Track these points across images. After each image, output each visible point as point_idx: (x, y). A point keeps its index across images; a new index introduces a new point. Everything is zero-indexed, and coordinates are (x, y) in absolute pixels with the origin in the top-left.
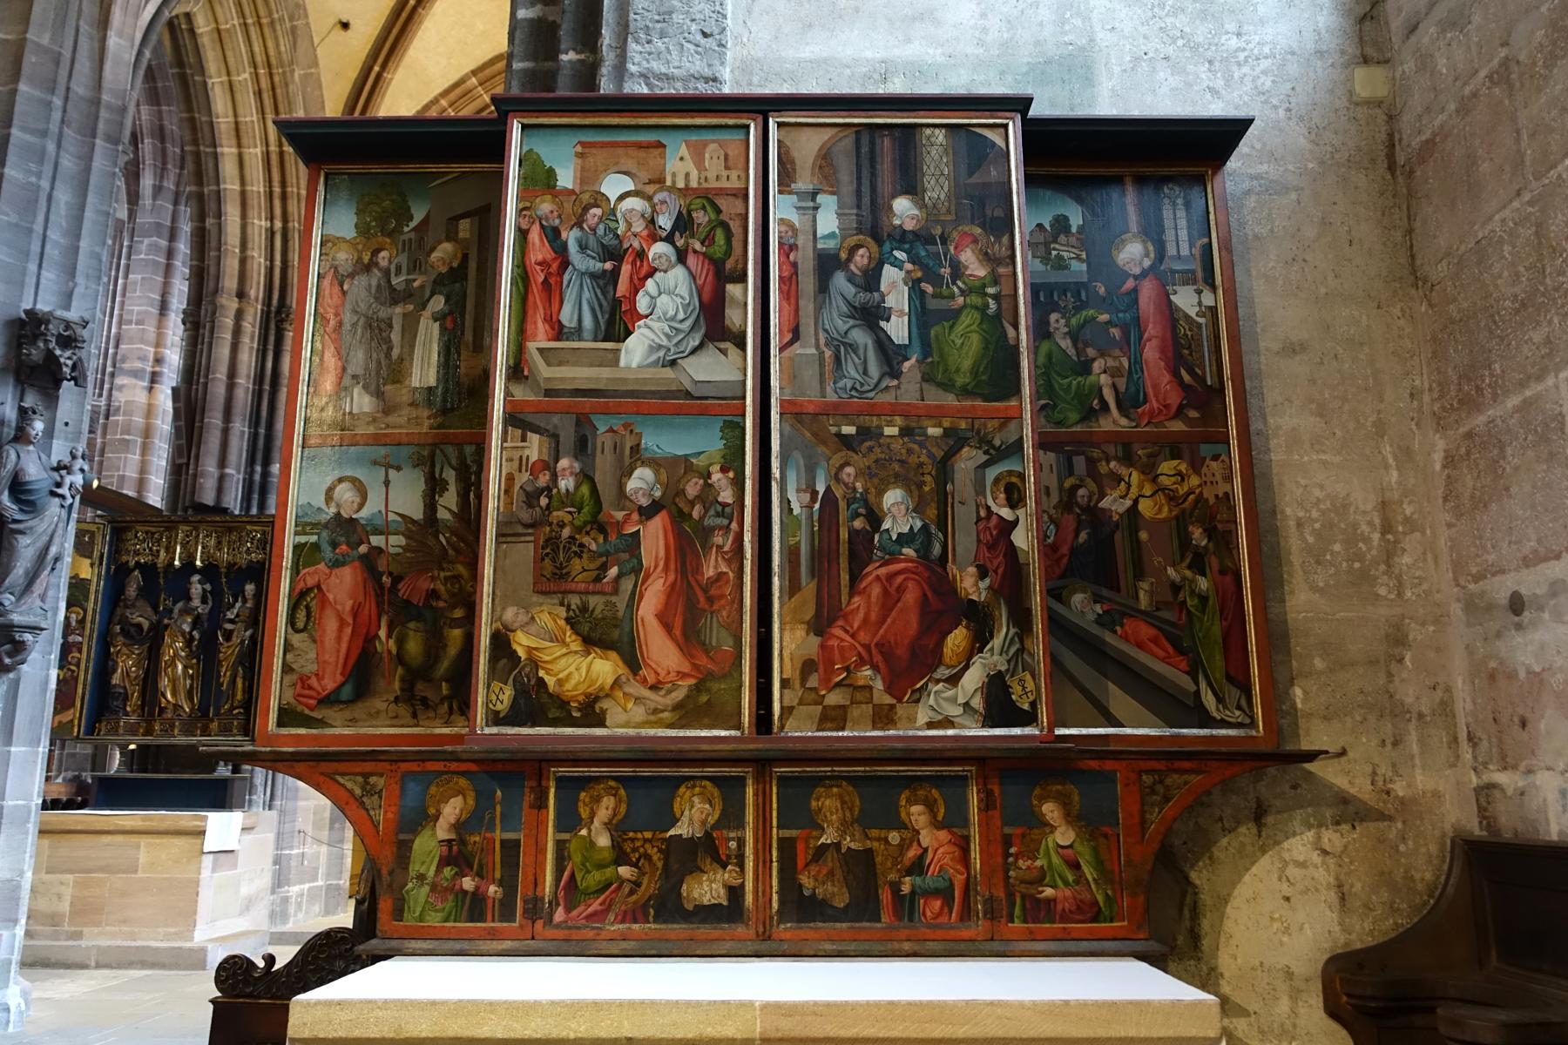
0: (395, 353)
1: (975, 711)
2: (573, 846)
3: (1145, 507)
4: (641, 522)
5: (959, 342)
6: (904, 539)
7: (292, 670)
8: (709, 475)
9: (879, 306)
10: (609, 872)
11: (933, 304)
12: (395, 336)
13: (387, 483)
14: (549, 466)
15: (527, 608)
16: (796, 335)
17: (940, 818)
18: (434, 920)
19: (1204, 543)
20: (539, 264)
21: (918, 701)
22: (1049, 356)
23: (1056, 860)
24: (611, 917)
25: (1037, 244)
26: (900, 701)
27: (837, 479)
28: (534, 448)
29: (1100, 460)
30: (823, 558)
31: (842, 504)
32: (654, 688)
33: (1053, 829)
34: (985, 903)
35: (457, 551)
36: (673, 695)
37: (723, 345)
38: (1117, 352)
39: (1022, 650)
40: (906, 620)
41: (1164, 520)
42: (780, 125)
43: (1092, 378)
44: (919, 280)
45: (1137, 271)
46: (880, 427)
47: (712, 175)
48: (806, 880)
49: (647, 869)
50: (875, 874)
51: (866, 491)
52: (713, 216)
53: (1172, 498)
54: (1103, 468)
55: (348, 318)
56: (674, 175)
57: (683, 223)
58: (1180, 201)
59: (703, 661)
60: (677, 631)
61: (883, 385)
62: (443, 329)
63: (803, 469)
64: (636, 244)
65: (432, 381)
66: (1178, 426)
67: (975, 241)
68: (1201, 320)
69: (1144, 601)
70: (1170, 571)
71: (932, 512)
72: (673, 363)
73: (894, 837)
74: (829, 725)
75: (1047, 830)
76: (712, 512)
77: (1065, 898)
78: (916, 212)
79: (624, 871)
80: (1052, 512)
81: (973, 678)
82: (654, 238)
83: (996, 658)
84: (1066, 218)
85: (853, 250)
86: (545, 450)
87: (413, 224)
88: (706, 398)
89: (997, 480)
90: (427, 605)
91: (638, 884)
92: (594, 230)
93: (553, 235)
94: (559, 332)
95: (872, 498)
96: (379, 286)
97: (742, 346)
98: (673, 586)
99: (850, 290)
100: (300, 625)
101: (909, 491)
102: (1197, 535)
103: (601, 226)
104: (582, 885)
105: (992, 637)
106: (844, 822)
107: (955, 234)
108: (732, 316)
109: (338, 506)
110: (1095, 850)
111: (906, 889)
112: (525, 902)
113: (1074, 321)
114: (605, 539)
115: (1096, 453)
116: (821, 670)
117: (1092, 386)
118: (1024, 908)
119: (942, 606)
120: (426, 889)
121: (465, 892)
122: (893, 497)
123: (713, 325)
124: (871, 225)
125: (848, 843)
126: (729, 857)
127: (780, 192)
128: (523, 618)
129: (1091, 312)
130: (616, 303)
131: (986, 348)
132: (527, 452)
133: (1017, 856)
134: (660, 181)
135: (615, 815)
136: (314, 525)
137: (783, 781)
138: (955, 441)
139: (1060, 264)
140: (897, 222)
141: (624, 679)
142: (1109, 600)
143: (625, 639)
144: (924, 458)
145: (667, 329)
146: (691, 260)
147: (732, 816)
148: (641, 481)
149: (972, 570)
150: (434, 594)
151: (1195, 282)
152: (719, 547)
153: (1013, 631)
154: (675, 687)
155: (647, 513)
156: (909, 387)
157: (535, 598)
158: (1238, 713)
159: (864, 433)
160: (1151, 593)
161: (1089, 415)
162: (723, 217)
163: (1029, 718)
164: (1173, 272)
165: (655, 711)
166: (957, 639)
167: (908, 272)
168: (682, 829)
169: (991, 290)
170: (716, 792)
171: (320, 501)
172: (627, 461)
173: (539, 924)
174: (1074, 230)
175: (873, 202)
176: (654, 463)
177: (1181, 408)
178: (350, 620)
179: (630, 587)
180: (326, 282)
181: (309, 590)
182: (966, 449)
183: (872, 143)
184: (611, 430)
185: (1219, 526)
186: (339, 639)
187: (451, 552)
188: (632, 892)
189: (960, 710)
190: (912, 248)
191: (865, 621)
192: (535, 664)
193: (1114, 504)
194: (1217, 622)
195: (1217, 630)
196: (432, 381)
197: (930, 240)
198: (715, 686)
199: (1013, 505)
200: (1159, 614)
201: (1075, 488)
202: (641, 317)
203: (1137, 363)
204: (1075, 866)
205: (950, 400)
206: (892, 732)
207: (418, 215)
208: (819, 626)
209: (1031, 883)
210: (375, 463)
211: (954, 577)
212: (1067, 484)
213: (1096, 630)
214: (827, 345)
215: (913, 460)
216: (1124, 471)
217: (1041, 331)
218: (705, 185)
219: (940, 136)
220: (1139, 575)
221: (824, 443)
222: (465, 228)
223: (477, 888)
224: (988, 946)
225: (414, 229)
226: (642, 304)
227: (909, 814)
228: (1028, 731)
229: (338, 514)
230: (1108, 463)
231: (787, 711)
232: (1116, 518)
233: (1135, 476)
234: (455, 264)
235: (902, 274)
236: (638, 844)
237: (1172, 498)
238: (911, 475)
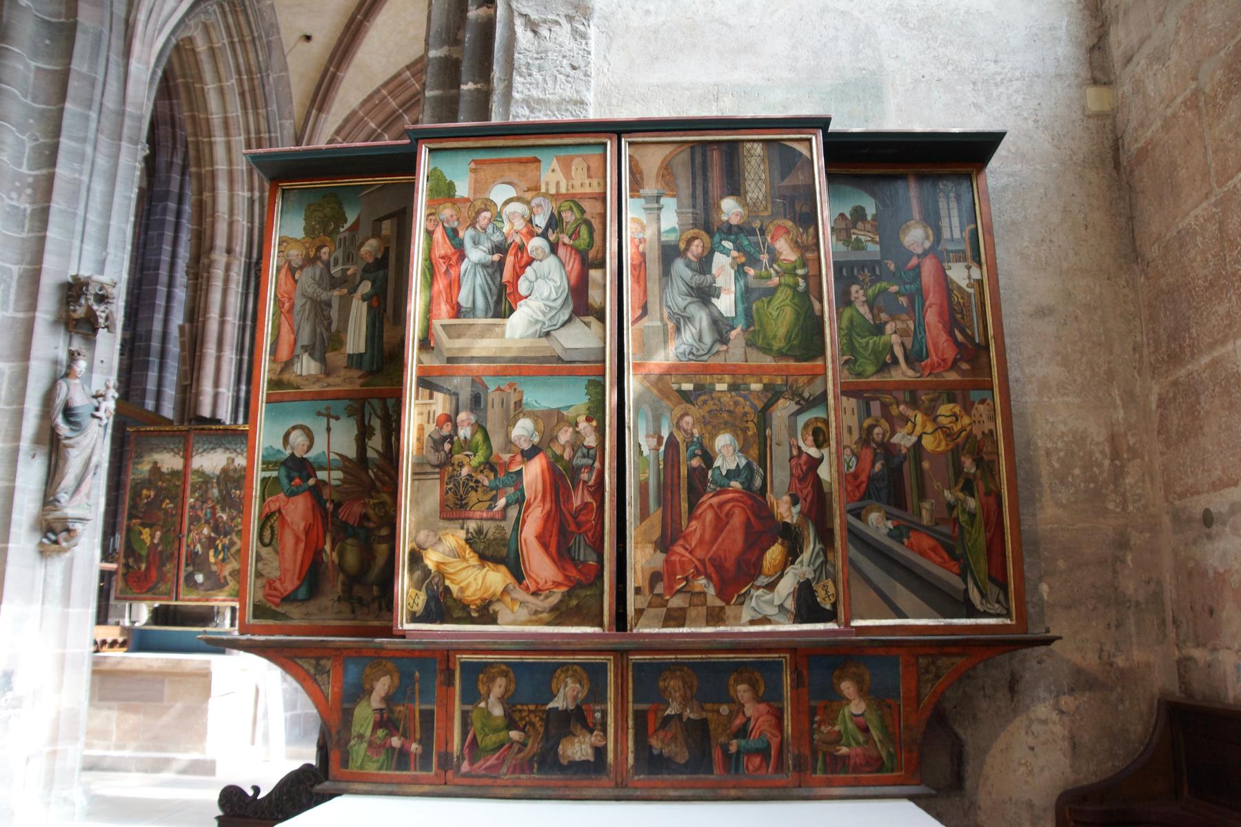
0: (334, 327)
1: (788, 611)
2: (475, 715)
3: (928, 442)
4: (523, 462)
5: (775, 314)
6: (731, 475)
7: (262, 575)
8: (577, 425)
9: (710, 286)
10: (502, 734)
11: (753, 283)
12: (334, 314)
13: (329, 429)
14: (450, 419)
15: (435, 530)
16: (645, 311)
17: (761, 693)
18: (372, 768)
19: (973, 471)
20: (443, 258)
21: (742, 604)
22: (851, 320)
23: (850, 726)
24: (504, 769)
25: (840, 230)
26: (728, 603)
27: (678, 426)
28: (440, 404)
29: (891, 404)
30: (667, 489)
31: (682, 447)
32: (535, 594)
33: (849, 701)
34: (794, 759)
36: (551, 599)
37: (587, 319)
38: (905, 317)
39: (825, 562)
40: (734, 540)
41: (942, 453)
42: (630, 144)
43: (884, 339)
44: (743, 265)
45: (919, 251)
46: (713, 384)
47: (577, 183)
48: (655, 743)
49: (532, 732)
50: (709, 739)
51: (702, 435)
52: (578, 215)
53: (949, 434)
54: (894, 411)
55: (299, 302)
56: (547, 184)
57: (555, 222)
58: (952, 195)
59: (573, 573)
60: (553, 549)
61: (715, 350)
62: (370, 308)
63: (651, 419)
64: (518, 240)
65: (362, 350)
66: (952, 376)
67: (788, 232)
68: (971, 291)
69: (926, 518)
70: (947, 493)
71: (754, 452)
72: (548, 334)
73: (724, 710)
74: (672, 623)
75: (844, 702)
76: (579, 454)
77: (857, 755)
78: (740, 210)
79: (514, 735)
80: (854, 447)
81: (787, 585)
82: (532, 234)
83: (805, 568)
84: (863, 209)
85: (689, 242)
86: (448, 406)
87: (347, 226)
88: (574, 362)
89: (806, 426)
90: (361, 525)
91: (524, 745)
92: (484, 229)
93: (453, 234)
94: (457, 311)
95: (706, 442)
96: (321, 275)
97: (601, 318)
98: (548, 515)
99: (687, 274)
100: (267, 540)
101: (736, 436)
102: (968, 465)
103: (490, 227)
104: (482, 744)
105: (802, 552)
106: (684, 698)
107: (771, 227)
108: (594, 296)
109: (293, 448)
110: (882, 719)
111: (733, 749)
112: (439, 756)
113: (870, 292)
114: (495, 476)
115: (888, 399)
116: (665, 579)
117: (885, 344)
118: (824, 762)
119: (764, 528)
120: (365, 745)
121: (394, 749)
122: (723, 441)
123: (580, 303)
124: (706, 222)
125: (689, 714)
126: (595, 725)
127: (631, 197)
128: (432, 539)
129: (884, 284)
130: (502, 288)
131: (797, 319)
132: (433, 407)
133: (820, 724)
134: (537, 188)
135: (506, 692)
136: (276, 464)
137: (638, 666)
138: (773, 394)
139: (859, 246)
140: (724, 218)
141: (511, 587)
142: (898, 517)
143: (512, 556)
144: (747, 409)
145: (543, 308)
146: (562, 251)
147: (597, 694)
148: (523, 430)
149: (786, 498)
150: (365, 517)
151: (965, 260)
152: (585, 482)
153: (818, 546)
154: (551, 593)
155: (529, 455)
156: (736, 352)
157: (442, 523)
158: (997, 606)
159: (699, 388)
160: (932, 512)
161: (883, 367)
162: (587, 216)
163: (831, 616)
164: (948, 252)
165: (536, 612)
166: (774, 553)
167: (734, 258)
168: (558, 703)
169: (800, 272)
170: (585, 676)
171: (279, 445)
172: (512, 413)
173: (450, 774)
174: (869, 218)
175: (706, 202)
176: (534, 415)
177: (955, 362)
178: (303, 537)
179: (515, 514)
180: (283, 271)
181: (273, 514)
182: (781, 401)
183: (704, 155)
184: (499, 389)
185: (985, 457)
186: (295, 551)
187: (378, 483)
188: (520, 751)
189: (777, 610)
190: (737, 239)
191: (701, 541)
192: (442, 575)
193: (903, 439)
194: (983, 534)
195: (982, 541)
196: (362, 350)
197: (752, 232)
198: (583, 593)
199: (819, 445)
200: (937, 528)
201: (872, 427)
202: (522, 298)
203: (921, 325)
204: (865, 730)
205: (768, 361)
206: (722, 629)
207: (351, 218)
208: (665, 544)
209: (831, 743)
210: (319, 414)
211: (772, 504)
212: (866, 424)
213: (889, 542)
214: (669, 318)
215: (739, 410)
216: (910, 413)
217: (844, 300)
218: (572, 191)
219: (758, 149)
220: (922, 496)
221: (668, 398)
222: (387, 227)
223: (403, 746)
224: (796, 792)
225: (348, 230)
226: (523, 287)
227: (736, 691)
228: (831, 626)
229: (293, 455)
230: (898, 405)
231: (639, 612)
232: (904, 451)
233: (920, 418)
234: (379, 256)
235: (729, 260)
236: (524, 714)
237: (949, 434)
238: (737, 423)
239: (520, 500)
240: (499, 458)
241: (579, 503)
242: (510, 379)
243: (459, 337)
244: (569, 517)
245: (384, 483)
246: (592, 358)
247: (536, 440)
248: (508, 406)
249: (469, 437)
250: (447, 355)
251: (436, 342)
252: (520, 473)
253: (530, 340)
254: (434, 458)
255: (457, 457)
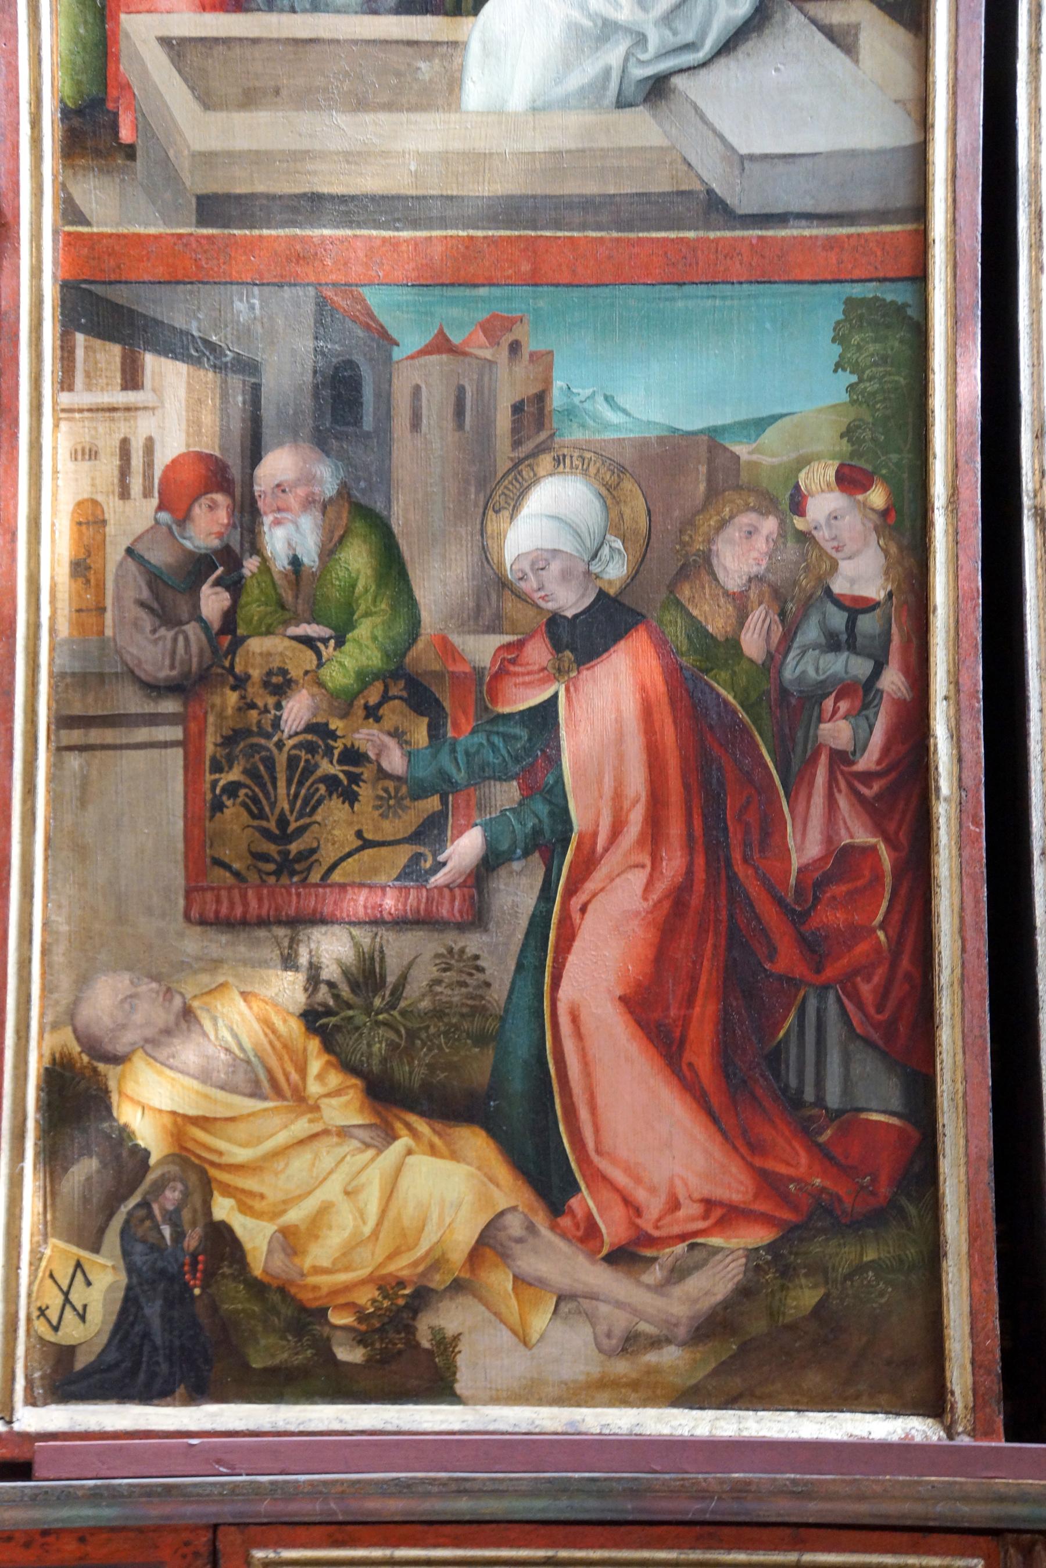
4: (560, 672)
8: (798, 504)
14: (224, 476)
15: (164, 976)
28: (176, 411)
32: (624, 1257)
59: (795, 1162)
60: (701, 1056)
72: (657, 90)
76: (811, 633)
86: (209, 419)
88: (782, 219)
98: (678, 900)
114: (435, 732)
132: (144, 427)
141: (514, 1225)
143: (517, 1083)
148: (550, 520)
152: (840, 758)
154: (698, 1255)
155: (587, 634)
157: (193, 943)
165: (632, 1343)
184: (441, 345)
192: (196, 1170)
198: (845, 1254)
239: (548, 838)
240: (446, 649)
241: (814, 849)
242: (490, 300)
243: (250, 99)
244: (770, 913)
246: (865, 200)
247: (615, 571)
248: (485, 424)
249: (310, 557)
250: (197, 183)
251: (141, 125)
252: (544, 718)
253: (575, 119)
254: (152, 651)
255: (262, 650)
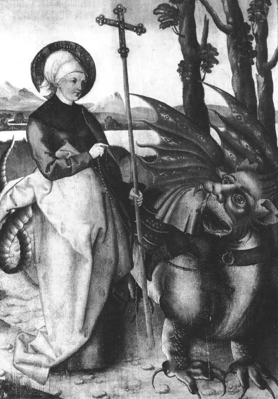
13: (124, 52)
35: (241, 154)
109: (53, 87)
181: (19, 212)
187: (228, 153)
229: (53, 100)
245: (241, 154)
